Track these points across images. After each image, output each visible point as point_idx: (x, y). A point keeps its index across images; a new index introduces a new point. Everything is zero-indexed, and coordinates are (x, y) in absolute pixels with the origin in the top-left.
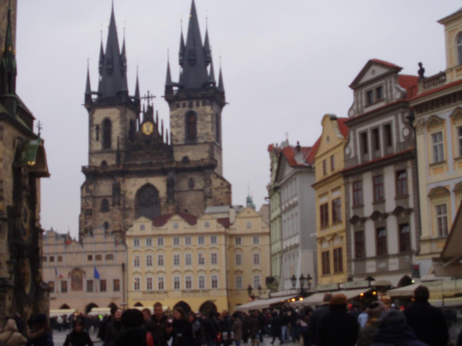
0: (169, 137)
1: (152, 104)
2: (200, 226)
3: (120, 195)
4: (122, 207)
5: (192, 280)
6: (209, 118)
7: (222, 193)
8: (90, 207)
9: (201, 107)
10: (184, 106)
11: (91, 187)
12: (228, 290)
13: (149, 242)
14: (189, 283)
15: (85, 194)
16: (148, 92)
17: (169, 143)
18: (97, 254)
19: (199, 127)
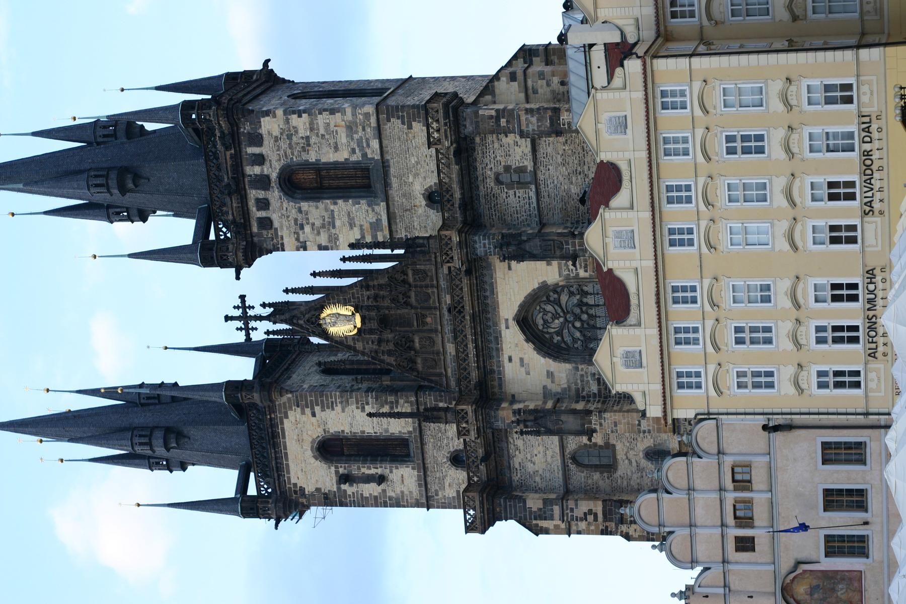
0: (367, 252)
1: (264, 305)
2: (623, 149)
3: (554, 411)
4: (592, 407)
5: (822, 179)
6: (300, 123)
7: (541, 75)
8: (598, 508)
9: (266, 149)
10: (264, 204)
11: (534, 503)
12: (859, 46)
13: (686, 336)
14: (838, 192)
15: (559, 523)
16: (227, 318)
17: (388, 252)
18: (730, 520)
19: (330, 157)
